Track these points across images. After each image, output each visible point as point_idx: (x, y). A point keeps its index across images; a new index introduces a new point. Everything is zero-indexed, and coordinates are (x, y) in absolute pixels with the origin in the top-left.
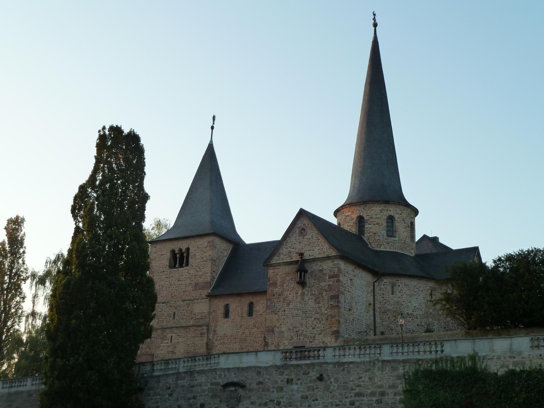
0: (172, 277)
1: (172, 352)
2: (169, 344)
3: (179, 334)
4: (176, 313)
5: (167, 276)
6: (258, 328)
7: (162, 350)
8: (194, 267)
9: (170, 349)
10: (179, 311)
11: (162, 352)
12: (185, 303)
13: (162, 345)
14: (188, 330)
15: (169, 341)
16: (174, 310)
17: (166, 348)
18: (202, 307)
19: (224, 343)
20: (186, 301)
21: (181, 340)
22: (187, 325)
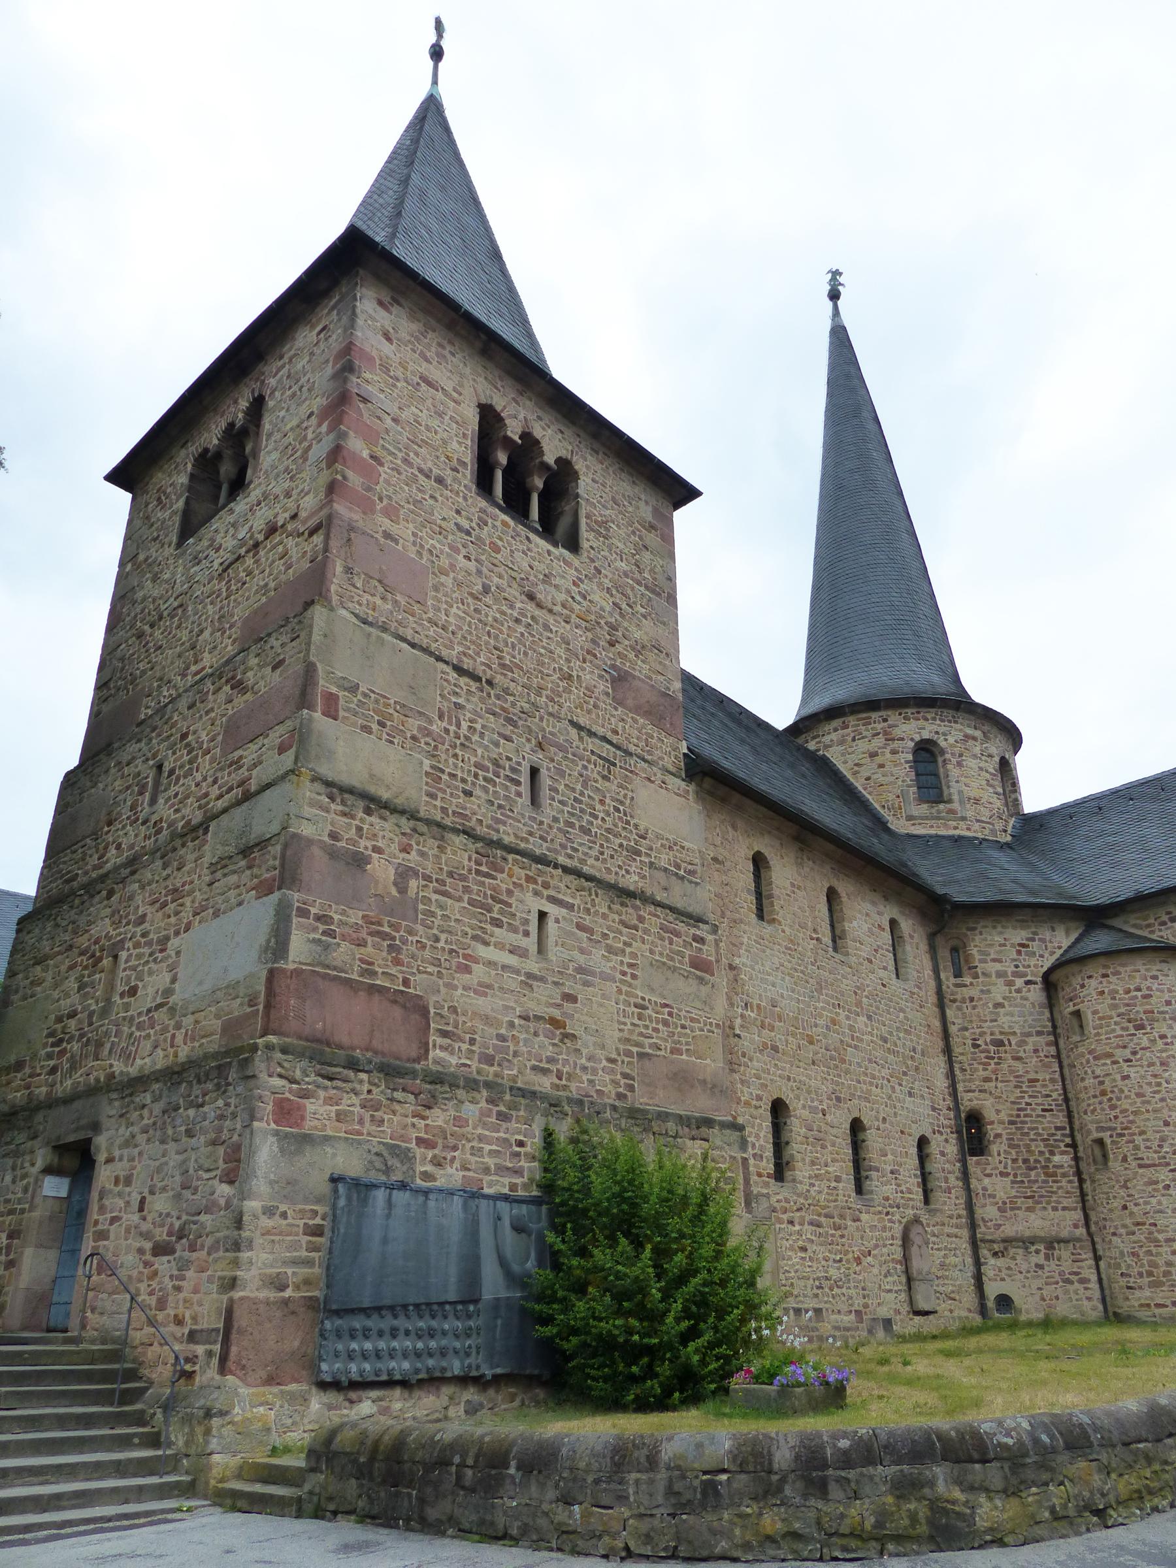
0: (497, 550)
1: (553, 1021)
2: (533, 965)
3: (588, 921)
4: (545, 780)
5: (465, 524)
6: (869, 1018)
7: (483, 989)
8: (607, 583)
9: (541, 1000)
10: (562, 773)
11: (483, 1004)
12: (591, 743)
13: (482, 951)
14: (630, 915)
15: (530, 943)
16: (528, 756)
17: (512, 981)
18: (670, 813)
19: (775, 1049)
20: (592, 734)
21: (597, 958)
22: (611, 879)
